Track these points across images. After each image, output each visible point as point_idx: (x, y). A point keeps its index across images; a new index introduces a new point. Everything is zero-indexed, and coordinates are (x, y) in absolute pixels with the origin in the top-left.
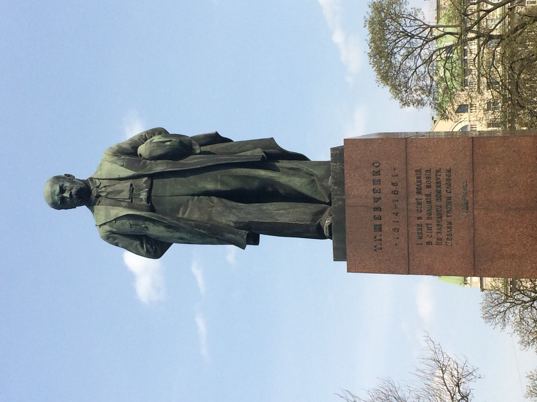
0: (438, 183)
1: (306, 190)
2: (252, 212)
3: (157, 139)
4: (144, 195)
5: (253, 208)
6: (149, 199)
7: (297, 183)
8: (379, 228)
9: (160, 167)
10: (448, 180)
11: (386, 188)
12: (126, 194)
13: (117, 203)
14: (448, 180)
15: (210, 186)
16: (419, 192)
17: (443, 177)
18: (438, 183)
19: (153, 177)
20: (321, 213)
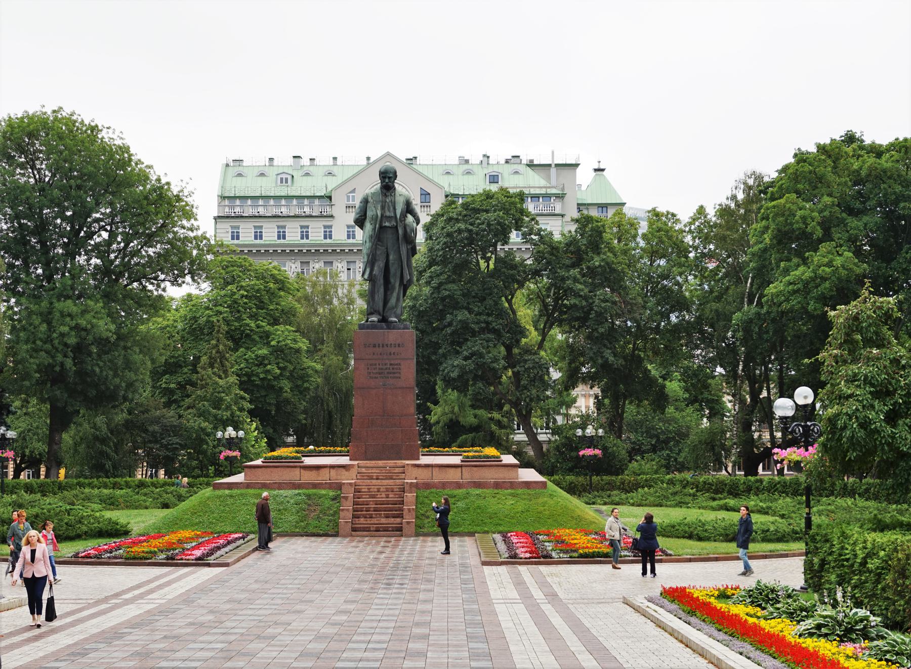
0: (394, 373)
1: (389, 305)
2: (381, 281)
3: (415, 225)
4: (387, 224)
5: (382, 281)
6: (386, 227)
7: (393, 301)
8: (374, 346)
9: (400, 232)
10: (397, 378)
11: (393, 350)
12: (388, 214)
13: (383, 208)
14: (397, 378)
15: (391, 257)
16: (391, 364)
17: (397, 375)
18: (394, 373)
19: (396, 227)
20: (379, 314)
